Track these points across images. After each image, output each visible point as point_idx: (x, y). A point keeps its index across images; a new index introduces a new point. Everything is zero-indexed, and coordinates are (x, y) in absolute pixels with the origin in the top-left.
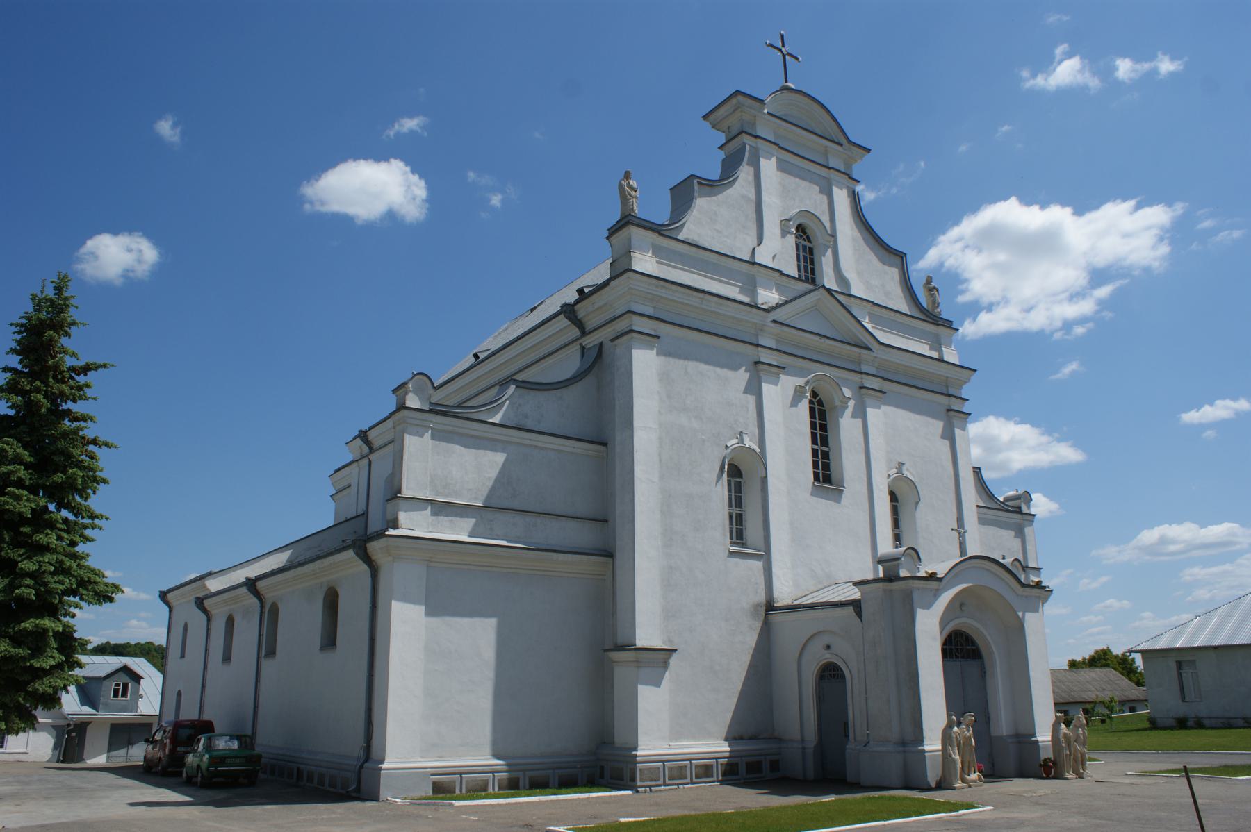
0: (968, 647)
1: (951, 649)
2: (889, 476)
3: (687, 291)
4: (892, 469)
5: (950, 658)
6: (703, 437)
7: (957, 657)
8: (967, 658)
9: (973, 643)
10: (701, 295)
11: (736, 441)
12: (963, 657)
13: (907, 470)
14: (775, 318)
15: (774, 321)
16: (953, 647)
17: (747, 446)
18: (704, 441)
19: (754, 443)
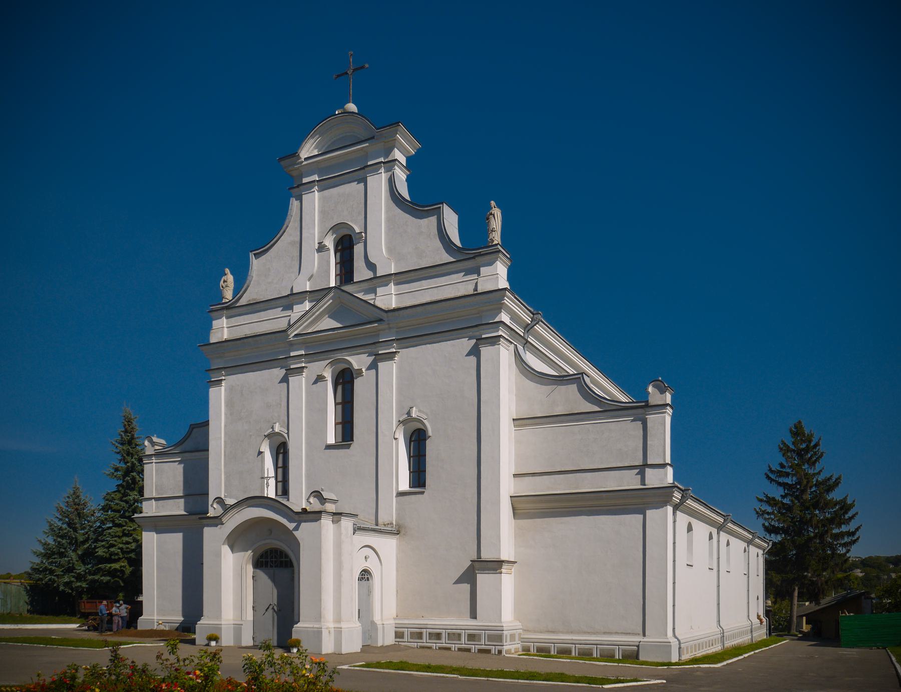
0: (282, 560)
1: (268, 562)
2: (399, 421)
3: (233, 343)
4: (403, 415)
5: (265, 567)
6: (251, 434)
7: (271, 566)
8: (280, 567)
9: (287, 556)
10: (242, 341)
11: (271, 430)
12: (275, 567)
13: (420, 411)
14: (296, 333)
15: (296, 335)
16: (269, 560)
17: (276, 431)
18: (251, 436)
19: (284, 428)
